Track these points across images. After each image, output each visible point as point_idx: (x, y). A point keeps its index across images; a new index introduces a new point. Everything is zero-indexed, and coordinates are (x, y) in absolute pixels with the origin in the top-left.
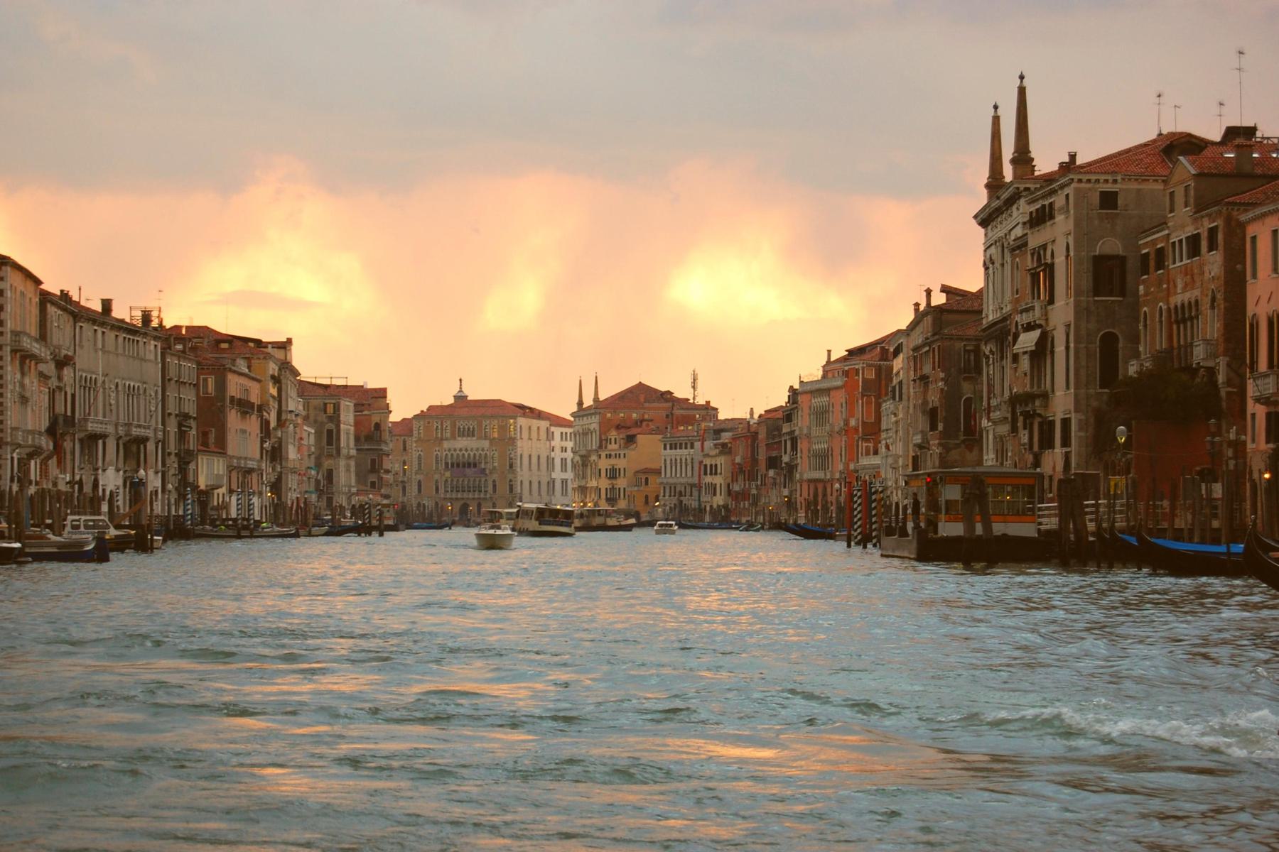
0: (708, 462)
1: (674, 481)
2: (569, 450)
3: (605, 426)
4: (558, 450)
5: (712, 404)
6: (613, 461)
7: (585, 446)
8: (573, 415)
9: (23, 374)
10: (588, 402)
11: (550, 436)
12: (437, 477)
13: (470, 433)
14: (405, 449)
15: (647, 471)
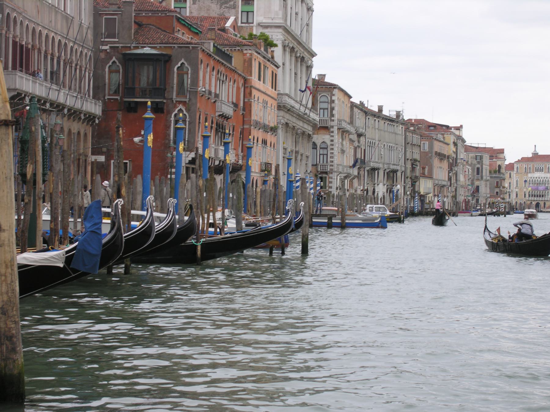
9: (343, 140)
12: (525, 190)
14: (510, 177)
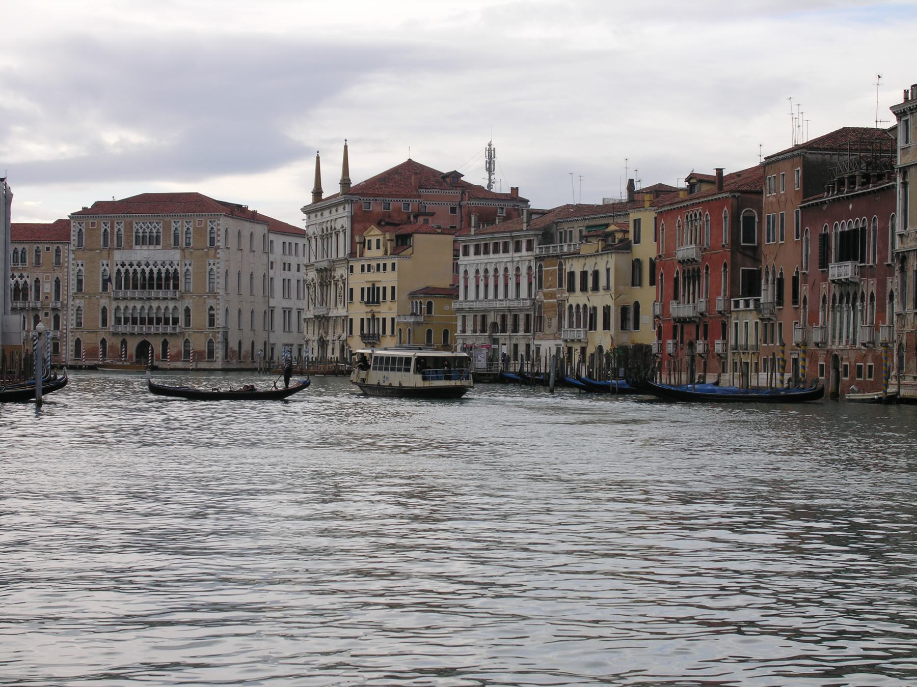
0: (576, 266)
1: (485, 305)
2: (294, 268)
3: (359, 220)
4: (278, 267)
5: (521, 194)
6: (373, 276)
7: (326, 252)
8: (307, 210)
10: (331, 188)
11: (268, 247)
12: (104, 302)
13: (154, 240)
15: (429, 292)
